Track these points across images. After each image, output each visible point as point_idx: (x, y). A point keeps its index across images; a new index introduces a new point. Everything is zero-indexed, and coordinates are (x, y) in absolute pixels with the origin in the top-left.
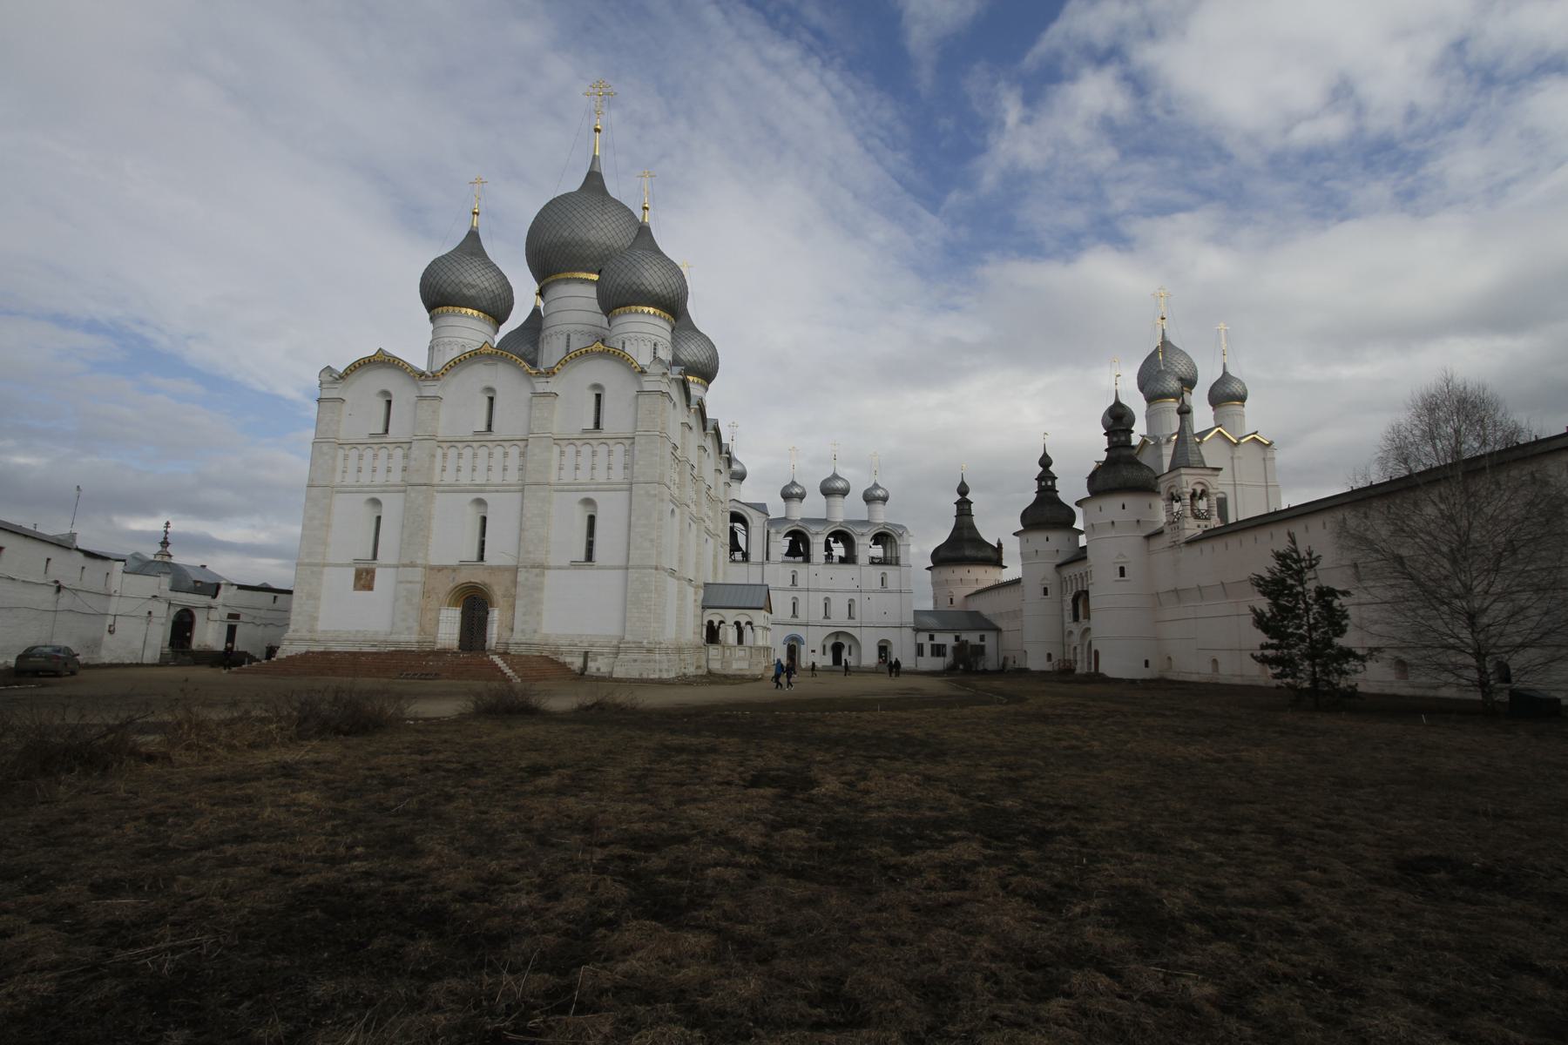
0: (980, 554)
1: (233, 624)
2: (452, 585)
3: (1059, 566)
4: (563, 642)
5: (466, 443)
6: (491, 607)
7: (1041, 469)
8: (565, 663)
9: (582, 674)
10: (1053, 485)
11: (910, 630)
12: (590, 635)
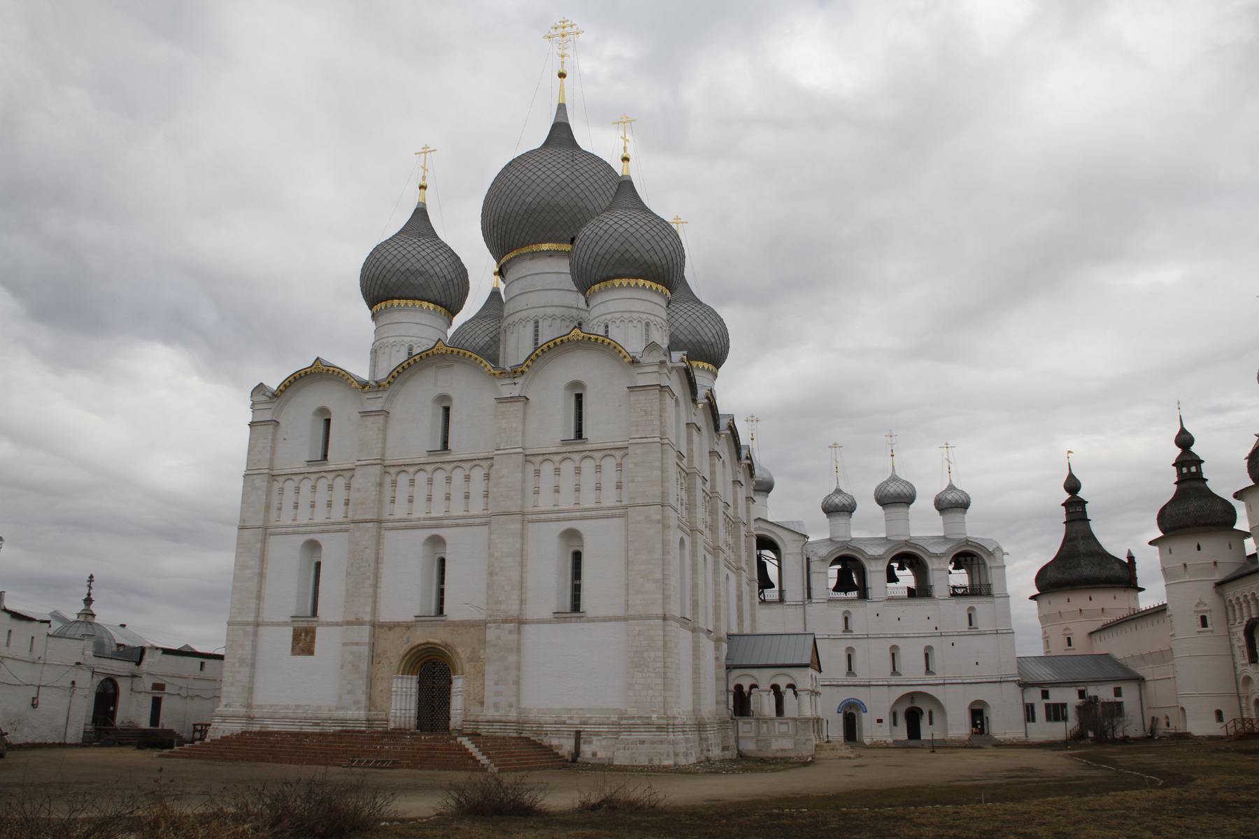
0: (1104, 573)
1: (159, 696)
2: (405, 648)
3: (1220, 585)
4: (547, 718)
5: (419, 467)
7: (1179, 451)
8: (552, 746)
9: (574, 760)
10: (1199, 472)
11: (1014, 685)
12: (582, 709)
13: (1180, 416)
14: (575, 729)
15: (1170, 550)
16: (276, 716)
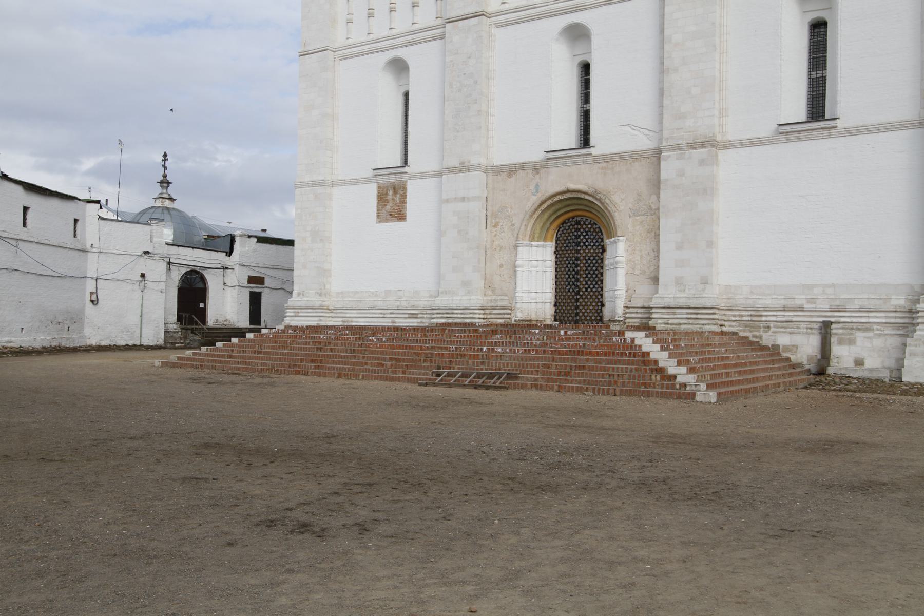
2: (535, 200)
4: (768, 302)
6: (609, 237)
8: (778, 346)
9: (821, 372)
14: (821, 319)
16: (361, 306)
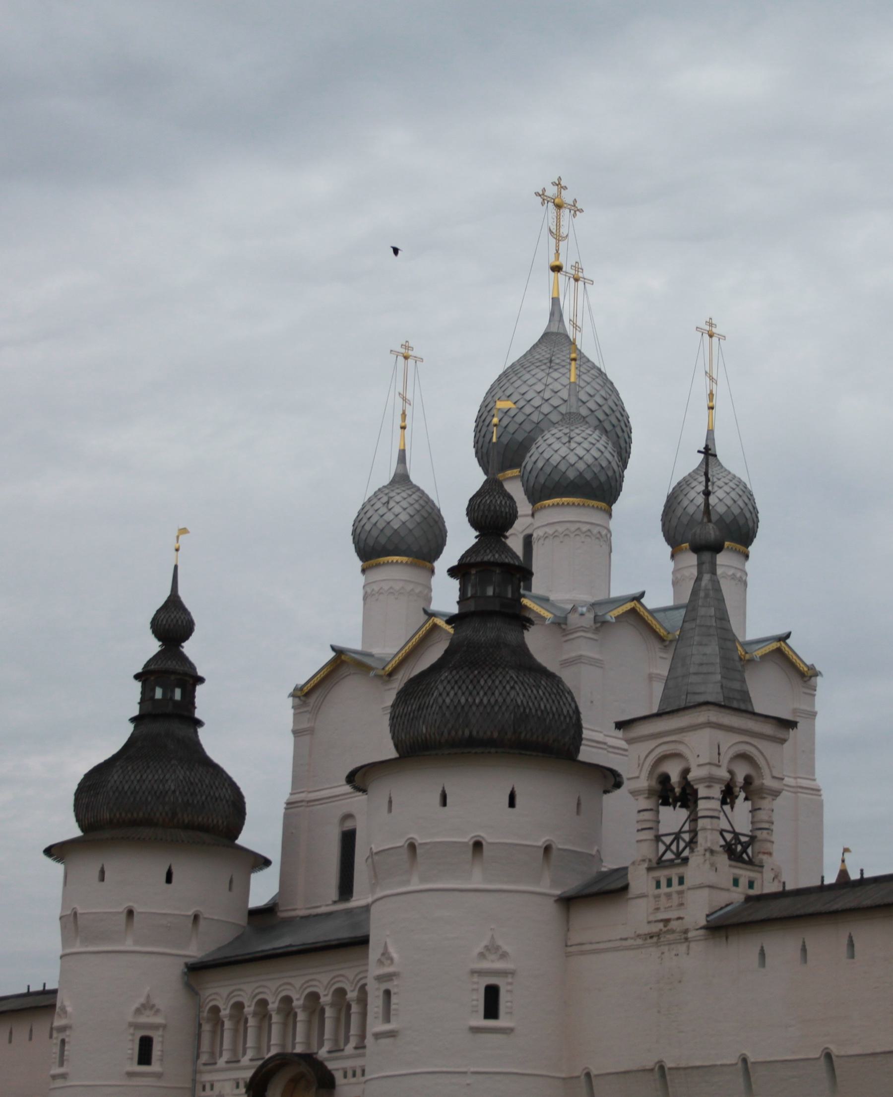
7: (154, 646)
13: (176, 567)
15: (102, 872)
